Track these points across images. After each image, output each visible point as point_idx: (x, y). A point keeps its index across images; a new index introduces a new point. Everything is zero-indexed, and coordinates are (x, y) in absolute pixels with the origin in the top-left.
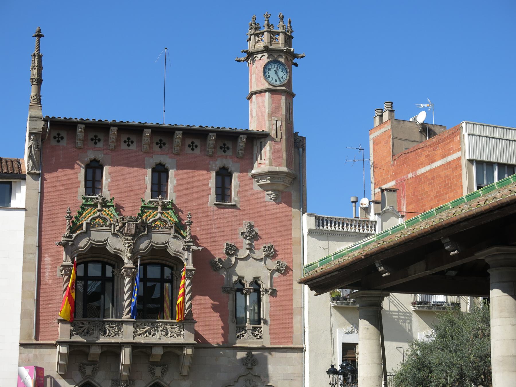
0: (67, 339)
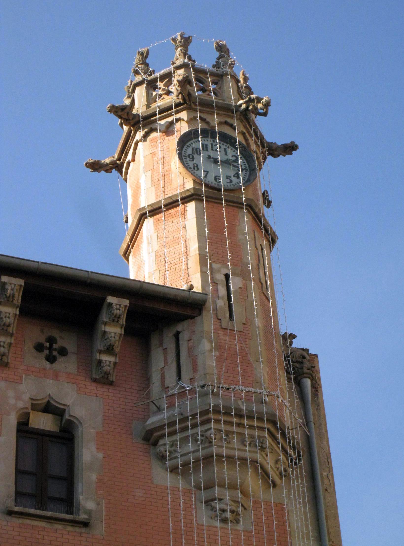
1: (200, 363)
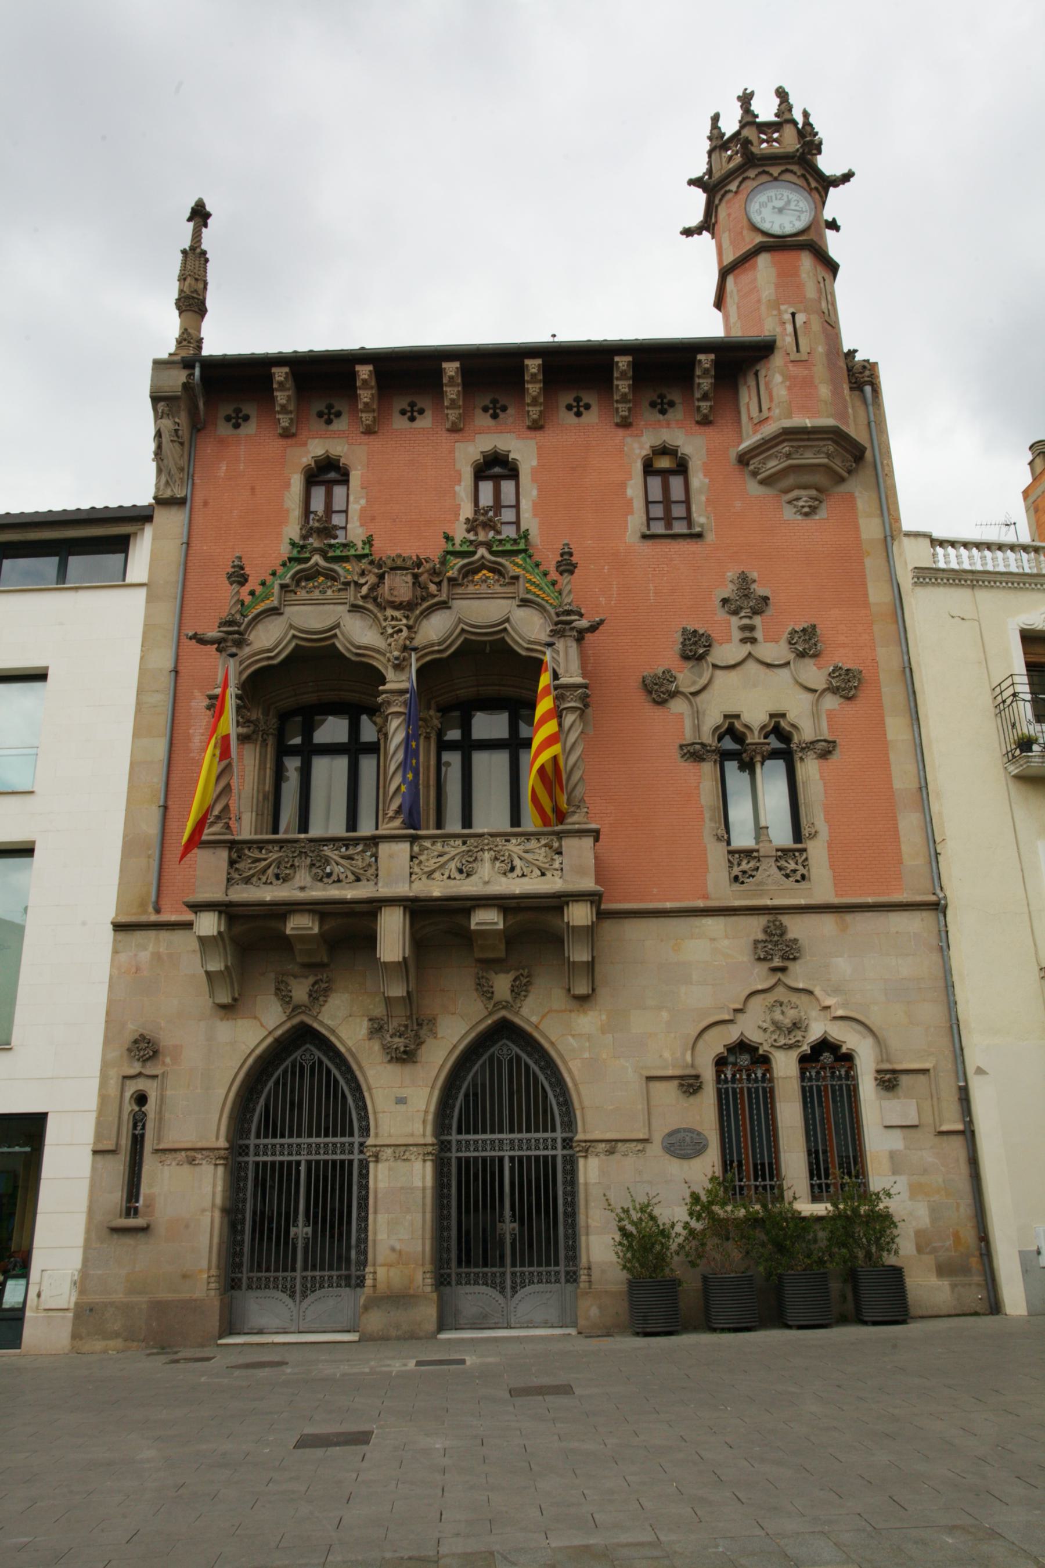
0: (216, 894)
1: (775, 393)
